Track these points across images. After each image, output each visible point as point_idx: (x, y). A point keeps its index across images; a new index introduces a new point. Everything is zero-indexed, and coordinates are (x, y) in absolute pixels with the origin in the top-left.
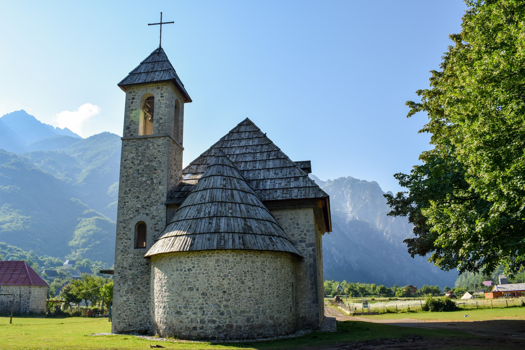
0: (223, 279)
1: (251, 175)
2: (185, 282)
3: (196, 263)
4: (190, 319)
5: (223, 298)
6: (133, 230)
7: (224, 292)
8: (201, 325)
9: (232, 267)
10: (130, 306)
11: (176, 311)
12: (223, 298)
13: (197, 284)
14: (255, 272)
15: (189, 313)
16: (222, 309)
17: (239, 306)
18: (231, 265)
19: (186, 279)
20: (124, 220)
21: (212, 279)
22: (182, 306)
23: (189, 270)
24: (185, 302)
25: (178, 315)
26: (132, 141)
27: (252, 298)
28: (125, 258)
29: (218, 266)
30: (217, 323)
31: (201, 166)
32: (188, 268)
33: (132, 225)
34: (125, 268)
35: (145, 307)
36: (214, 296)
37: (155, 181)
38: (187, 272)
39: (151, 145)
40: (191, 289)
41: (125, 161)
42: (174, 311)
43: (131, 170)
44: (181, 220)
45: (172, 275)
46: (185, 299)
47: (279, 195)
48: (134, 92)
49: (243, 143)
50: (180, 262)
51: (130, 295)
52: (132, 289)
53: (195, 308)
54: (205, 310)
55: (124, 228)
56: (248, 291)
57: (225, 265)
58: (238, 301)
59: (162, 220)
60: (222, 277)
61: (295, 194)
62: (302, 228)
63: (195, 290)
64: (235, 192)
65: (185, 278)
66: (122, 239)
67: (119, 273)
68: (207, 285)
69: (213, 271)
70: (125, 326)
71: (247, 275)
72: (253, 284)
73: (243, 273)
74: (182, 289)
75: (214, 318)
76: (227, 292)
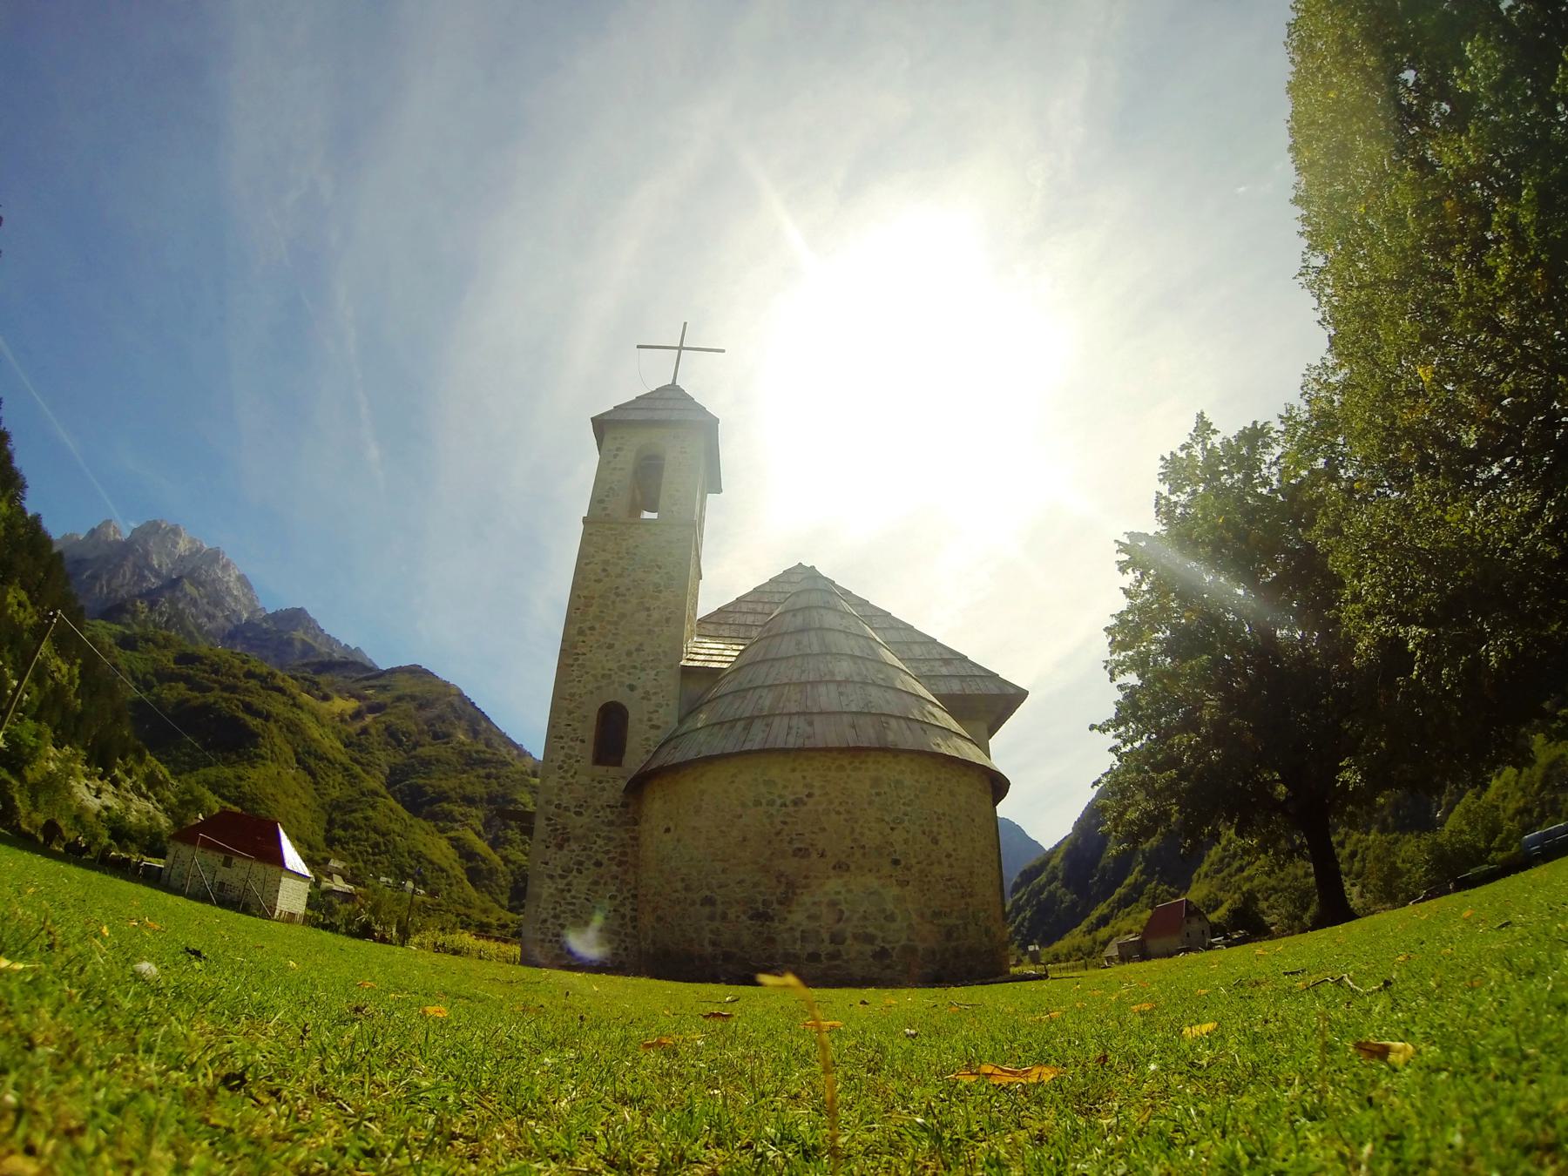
0: (892, 829)
2: (784, 833)
3: (817, 784)
4: (798, 934)
5: (891, 876)
7: (896, 862)
8: (831, 948)
9: (911, 800)
10: (574, 904)
11: (750, 912)
12: (891, 876)
14: (956, 818)
16: (890, 907)
17: (930, 899)
18: (909, 794)
19: (786, 827)
20: (572, 695)
21: (862, 827)
22: (774, 898)
23: (795, 803)
24: (782, 888)
25: (759, 923)
26: (607, 526)
27: (955, 882)
28: (567, 784)
29: (878, 794)
30: (879, 942)
32: (792, 797)
34: (567, 809)
35: (615, 911)
36: (870, 871)
38: (791, 809)
40: (801, 853)
41: (587, 564)
42: (744, 913)
44: (750, 688)
45: (741, 816)
46: (783, 879)
48: (622, 438)
50: (766, 783)
51: (575, 877)
52: (580, 863)
53: (814, 903)
54: (843, 908)
56: (946, 864)
57: (895, 794)
58: (926, 887)
59: (668, 705)
60: (888, 823)
63: (814, 856)
65: (785, 823)
66: (562, 738)
67: (550, 819)
68: (848, 842)
69: (866, 806)
70: (557, 951)
71: (943, 823)
72: (954, 846)
73: (935, 816)
74: (773, 854)
75: (871, 930)
76: (903, 863)
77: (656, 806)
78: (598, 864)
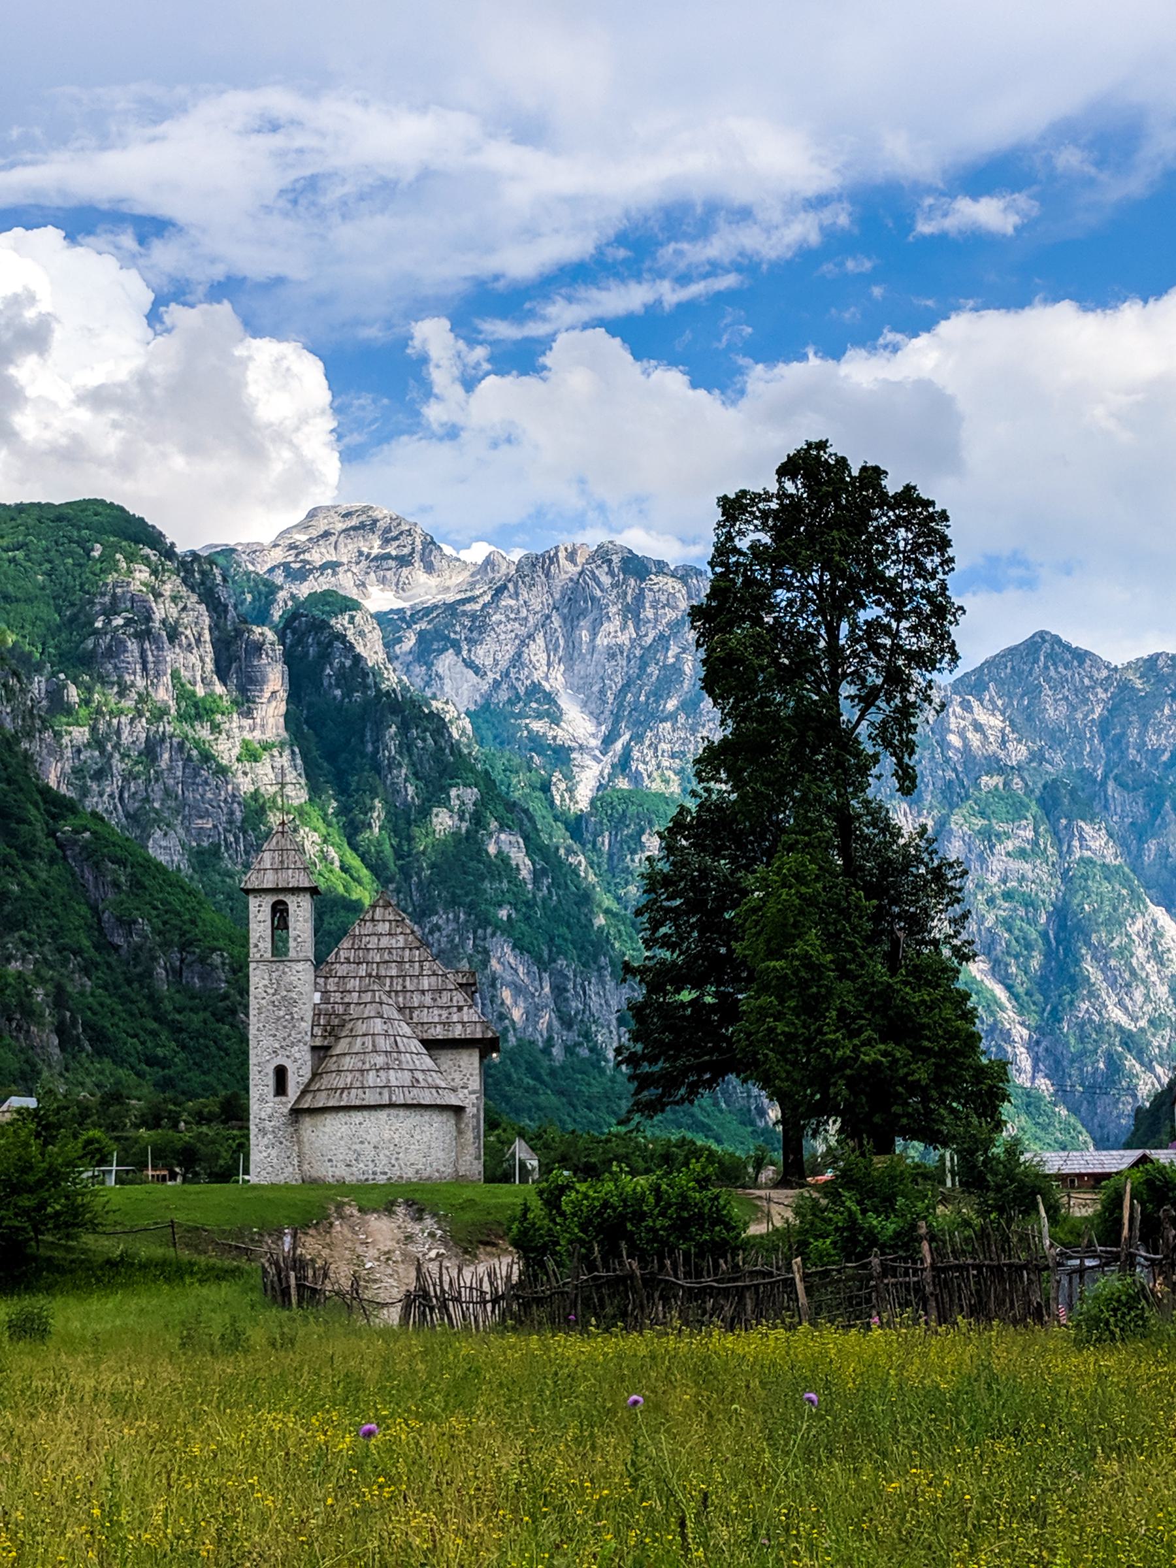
1: (401, 999)
6: (271, 1075)
15: (361, 1165)
16: (393, 1162)
31: (331, 980)
33: (270, 1069)
37: (296, 1016)
39: (287, 970)
40: (362, 1142)
43: (263, 1002)
47: (438, 1033)
49: (385, 942)
55: (260, 1072)
61: (457, 1032)
64: (398, 1038)
77: (307, 1122)
78: (281, 1143)
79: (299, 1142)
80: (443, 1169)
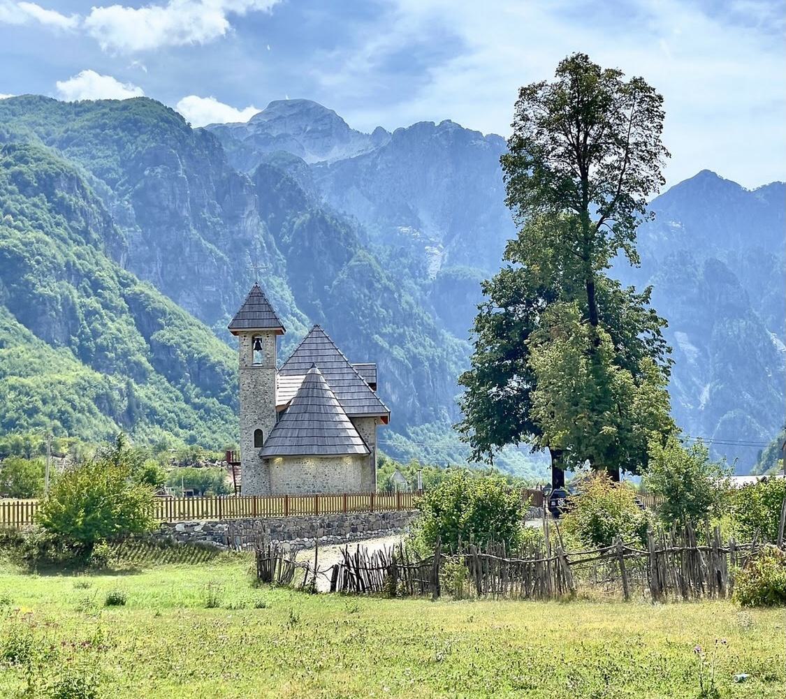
13: (310, 471)
16: (325, 485)
62: (366, 432)
79: (269, 473)
80: (354, 489)
